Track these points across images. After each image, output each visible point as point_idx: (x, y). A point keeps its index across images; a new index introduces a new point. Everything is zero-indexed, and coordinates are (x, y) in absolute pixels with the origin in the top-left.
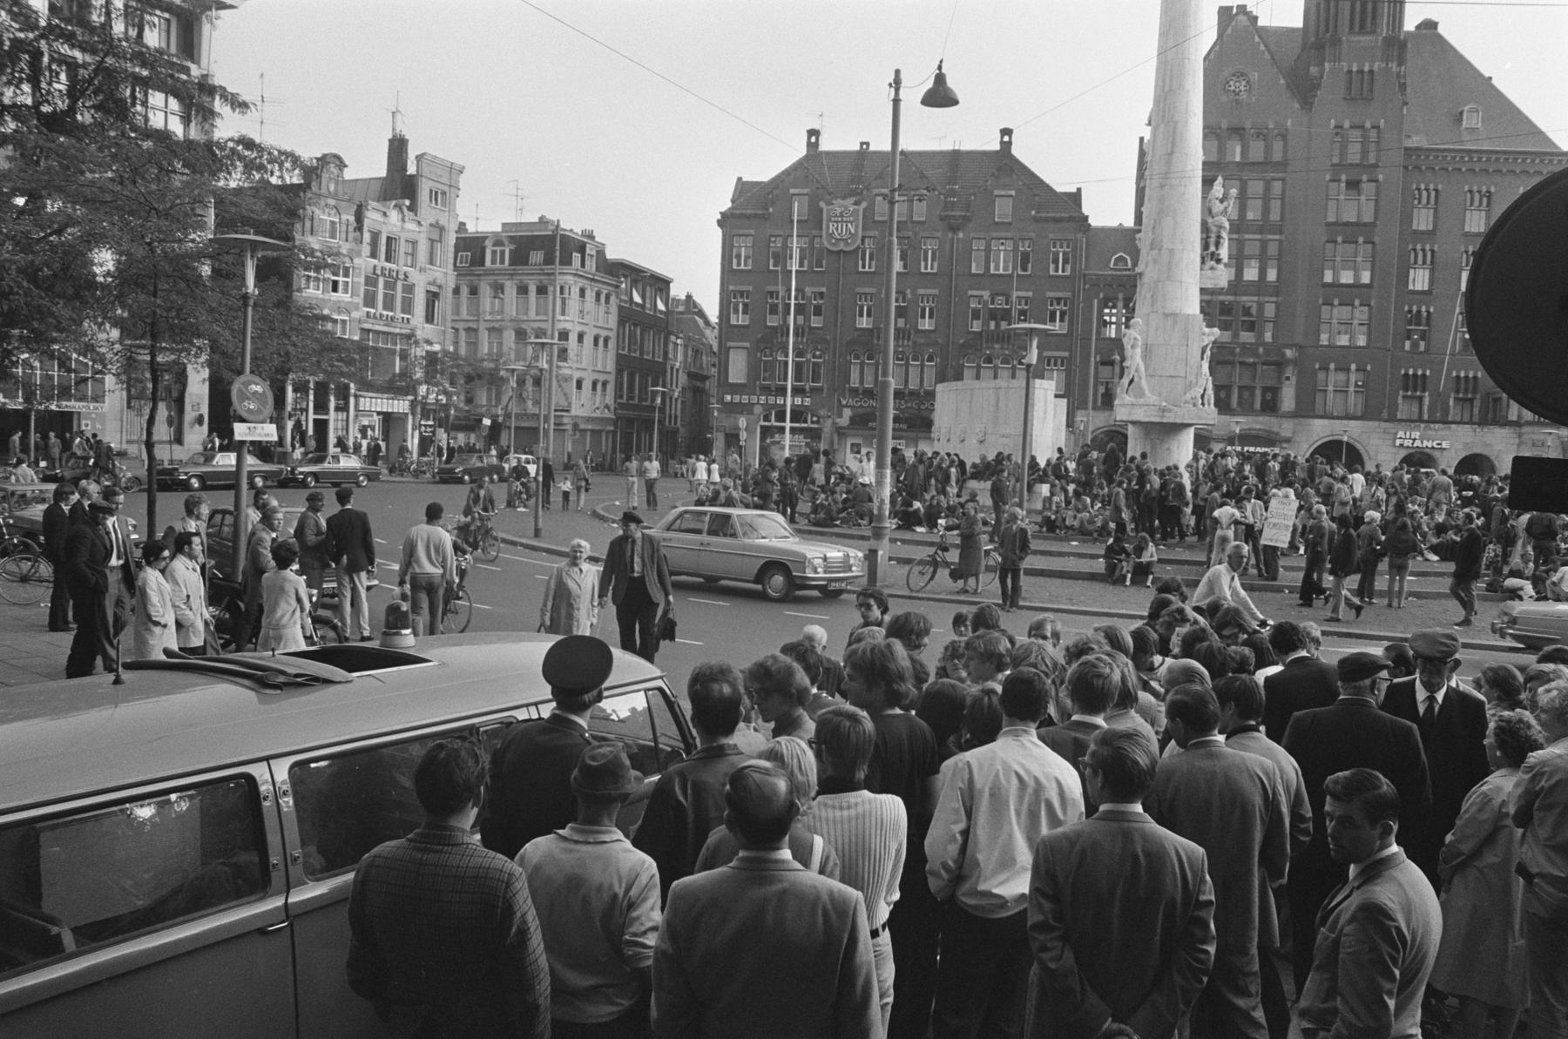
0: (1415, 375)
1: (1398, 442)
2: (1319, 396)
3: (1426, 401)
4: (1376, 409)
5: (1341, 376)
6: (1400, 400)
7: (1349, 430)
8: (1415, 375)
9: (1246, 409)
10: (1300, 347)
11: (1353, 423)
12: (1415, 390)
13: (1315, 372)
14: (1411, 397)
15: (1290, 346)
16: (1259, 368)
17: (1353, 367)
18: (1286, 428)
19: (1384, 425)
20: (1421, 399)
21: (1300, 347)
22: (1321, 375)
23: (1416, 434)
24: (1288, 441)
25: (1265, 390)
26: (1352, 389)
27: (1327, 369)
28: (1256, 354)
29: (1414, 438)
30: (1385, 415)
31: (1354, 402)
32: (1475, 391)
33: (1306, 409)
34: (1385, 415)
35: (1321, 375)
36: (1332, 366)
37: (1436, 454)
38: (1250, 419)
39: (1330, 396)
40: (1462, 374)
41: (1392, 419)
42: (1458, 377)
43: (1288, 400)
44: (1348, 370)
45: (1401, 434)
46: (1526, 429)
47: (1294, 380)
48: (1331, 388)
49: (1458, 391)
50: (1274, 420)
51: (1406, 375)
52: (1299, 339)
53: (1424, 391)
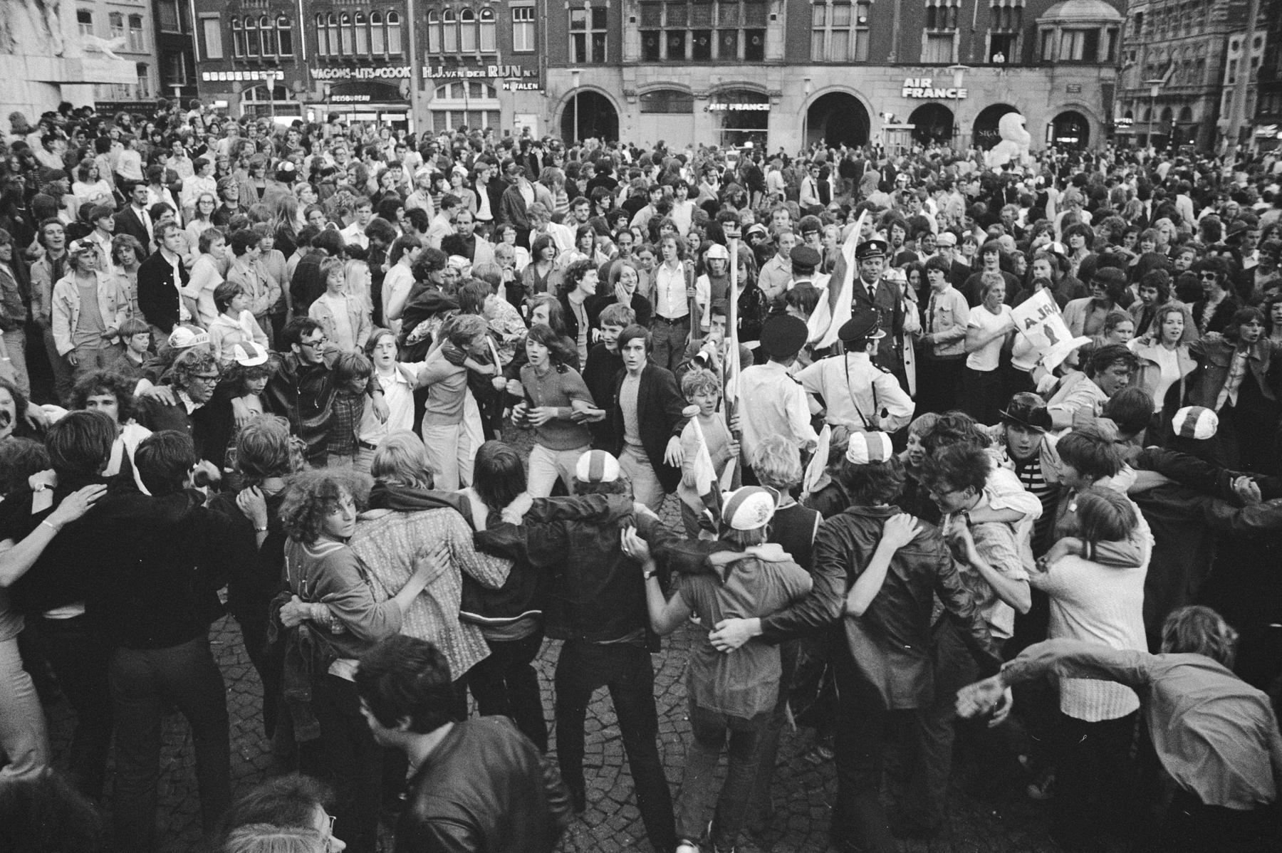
5: (841, 12)
7: (852, 80)
9: (728, 56)
18: (769, 79)
19: (890, 71)
20: (950, 37)
22: (818, 13)
23: (927, 82)
26: (853, 27)
31: (856, 44)
35: (818, 13)
37: (951, 106)
43: (775, 45)
45: (909, 82)
47: (782, 19)
48: (828, 28)
50: (759, 70)
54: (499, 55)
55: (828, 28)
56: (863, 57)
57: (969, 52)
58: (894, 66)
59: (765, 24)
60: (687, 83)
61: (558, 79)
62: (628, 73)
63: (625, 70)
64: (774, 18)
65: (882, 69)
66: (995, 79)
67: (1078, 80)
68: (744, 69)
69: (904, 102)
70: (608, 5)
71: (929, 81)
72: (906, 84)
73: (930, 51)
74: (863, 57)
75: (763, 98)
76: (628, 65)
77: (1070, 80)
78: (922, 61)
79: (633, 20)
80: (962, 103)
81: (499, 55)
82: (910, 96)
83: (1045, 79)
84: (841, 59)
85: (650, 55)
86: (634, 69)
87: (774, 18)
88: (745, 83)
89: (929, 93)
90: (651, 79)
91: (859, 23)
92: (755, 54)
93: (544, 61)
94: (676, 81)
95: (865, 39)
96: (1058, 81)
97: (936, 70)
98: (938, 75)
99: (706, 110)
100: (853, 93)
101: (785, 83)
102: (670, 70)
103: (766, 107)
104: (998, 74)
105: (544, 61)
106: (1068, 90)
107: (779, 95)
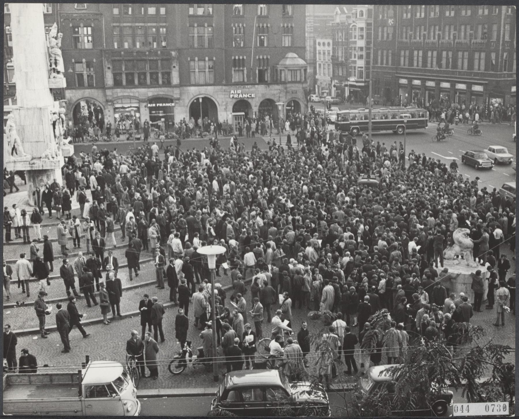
0: (239, 59)
1: (231, 96)
2: (192, 74)
3: (245, 72)
4: (222, 79)
5: (202, 63)
6: (233, 72)
7: (209, 91)
8: (239, 59)
9: (155, 84)
10: (179, 50)
11: (209, 88)
12: (239, 67)
13: (189, 62)
14: (238, 71)
15: (174, 50)
16: (159, 62)
17: (207, 59)
18: (175, 93)
19: (224, 87)
20: (243, 71)
21: (179, 50)
22: (192, 63)
23: (239, 91)
24: (179, 99)
25: (163, 74)
26: (207, 70)
27: (194, 60)
28: (156, 55)
29: (238, 93)
30: (224, 82)
31: (209, 77)
32: (268, 65)
33: (185, 81)
34: (224, 82)
35: (192, 63)
36: (196, 59)
37: (250, 101)
38: (157, 89)
39: (197, 74)
40: (261, 57)
41: (229, 83)
42: (259, 59)
43: (175, 79)
44: (205, 60)
45: (232, 92)
46: (288, 85)
47: (177, 68)
48: (197, 70)
49: (260, 66)
50: (170, 89)
51: (235, 59)
52: (179, 45)
53: (244, 66)
55: (197, 70)
58: (225, 85)
59: (170, 69)
61: (71, 95)
62: (109, 92)
64: (174, 67)
65: (221, 87)
68: (163, 89)
69: (230, 100)
70: (95, 60)
73: (236, 77)
75: (172, 101)
79: (109, 68)
84: (202, 82)
85: (117, 84)
87: (174, 67)
89: (241, 96)
90: (120, 94)
91: (209, 68)
92: (168, 83)
95: (212, 76)
100: (209, 97)
101: (181, 94)
102: (129, 90)
107: (179, 99)
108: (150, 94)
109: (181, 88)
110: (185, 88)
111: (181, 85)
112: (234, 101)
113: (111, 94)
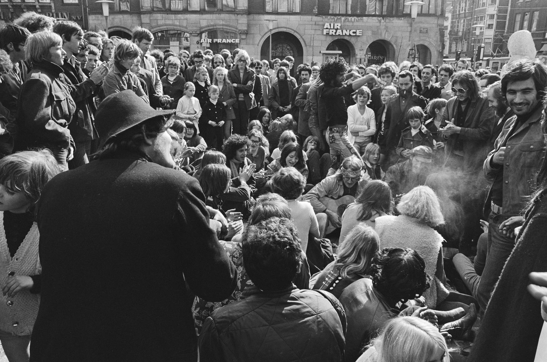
1: (325, 32)
19: (315, 18)
23: (338, 25)
24: (246, 33)
37: (352, 40)
45: (327, 25)
54: (53, 5)
56: (298, 10)
57: (357, 10)
60: (185, 25)
61: (96, 22)
63: (142, 16)
66: (378, 24)
67: (426, 26)
69: (323, 38)
71: (339, 25)
72: (325, 27)
74: (298, 10)
76: (145, 13)
77: (422, 25)
78: (330, 12)
80: (359, 39)
81: (53, 5)
82: (328, 34)
83: (408, 25)
86: (149, 15)
88: (223, 25)
89: (339, 32)
90: (160, 22)
93: (85, 10)
94: (178, 24)
96: (414, 26)
97: (343, 18)
98: (344, 21)
99: (198, 43)
100: (292, 32)
101: (249, 25)
103: (237, 41)
104: (380, 22)
105: (85, 10)
106: (421, 32)
108: (204, 23)
109: (251, 17)
110: (257, 17)
111: (249, 12)
112: (330, 40)
113: (148, 22)
